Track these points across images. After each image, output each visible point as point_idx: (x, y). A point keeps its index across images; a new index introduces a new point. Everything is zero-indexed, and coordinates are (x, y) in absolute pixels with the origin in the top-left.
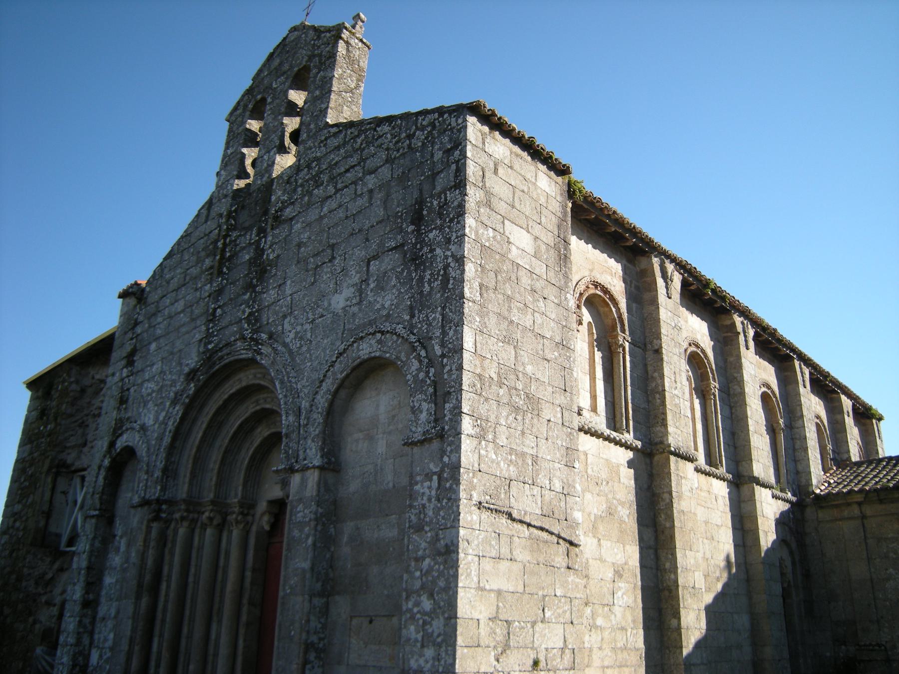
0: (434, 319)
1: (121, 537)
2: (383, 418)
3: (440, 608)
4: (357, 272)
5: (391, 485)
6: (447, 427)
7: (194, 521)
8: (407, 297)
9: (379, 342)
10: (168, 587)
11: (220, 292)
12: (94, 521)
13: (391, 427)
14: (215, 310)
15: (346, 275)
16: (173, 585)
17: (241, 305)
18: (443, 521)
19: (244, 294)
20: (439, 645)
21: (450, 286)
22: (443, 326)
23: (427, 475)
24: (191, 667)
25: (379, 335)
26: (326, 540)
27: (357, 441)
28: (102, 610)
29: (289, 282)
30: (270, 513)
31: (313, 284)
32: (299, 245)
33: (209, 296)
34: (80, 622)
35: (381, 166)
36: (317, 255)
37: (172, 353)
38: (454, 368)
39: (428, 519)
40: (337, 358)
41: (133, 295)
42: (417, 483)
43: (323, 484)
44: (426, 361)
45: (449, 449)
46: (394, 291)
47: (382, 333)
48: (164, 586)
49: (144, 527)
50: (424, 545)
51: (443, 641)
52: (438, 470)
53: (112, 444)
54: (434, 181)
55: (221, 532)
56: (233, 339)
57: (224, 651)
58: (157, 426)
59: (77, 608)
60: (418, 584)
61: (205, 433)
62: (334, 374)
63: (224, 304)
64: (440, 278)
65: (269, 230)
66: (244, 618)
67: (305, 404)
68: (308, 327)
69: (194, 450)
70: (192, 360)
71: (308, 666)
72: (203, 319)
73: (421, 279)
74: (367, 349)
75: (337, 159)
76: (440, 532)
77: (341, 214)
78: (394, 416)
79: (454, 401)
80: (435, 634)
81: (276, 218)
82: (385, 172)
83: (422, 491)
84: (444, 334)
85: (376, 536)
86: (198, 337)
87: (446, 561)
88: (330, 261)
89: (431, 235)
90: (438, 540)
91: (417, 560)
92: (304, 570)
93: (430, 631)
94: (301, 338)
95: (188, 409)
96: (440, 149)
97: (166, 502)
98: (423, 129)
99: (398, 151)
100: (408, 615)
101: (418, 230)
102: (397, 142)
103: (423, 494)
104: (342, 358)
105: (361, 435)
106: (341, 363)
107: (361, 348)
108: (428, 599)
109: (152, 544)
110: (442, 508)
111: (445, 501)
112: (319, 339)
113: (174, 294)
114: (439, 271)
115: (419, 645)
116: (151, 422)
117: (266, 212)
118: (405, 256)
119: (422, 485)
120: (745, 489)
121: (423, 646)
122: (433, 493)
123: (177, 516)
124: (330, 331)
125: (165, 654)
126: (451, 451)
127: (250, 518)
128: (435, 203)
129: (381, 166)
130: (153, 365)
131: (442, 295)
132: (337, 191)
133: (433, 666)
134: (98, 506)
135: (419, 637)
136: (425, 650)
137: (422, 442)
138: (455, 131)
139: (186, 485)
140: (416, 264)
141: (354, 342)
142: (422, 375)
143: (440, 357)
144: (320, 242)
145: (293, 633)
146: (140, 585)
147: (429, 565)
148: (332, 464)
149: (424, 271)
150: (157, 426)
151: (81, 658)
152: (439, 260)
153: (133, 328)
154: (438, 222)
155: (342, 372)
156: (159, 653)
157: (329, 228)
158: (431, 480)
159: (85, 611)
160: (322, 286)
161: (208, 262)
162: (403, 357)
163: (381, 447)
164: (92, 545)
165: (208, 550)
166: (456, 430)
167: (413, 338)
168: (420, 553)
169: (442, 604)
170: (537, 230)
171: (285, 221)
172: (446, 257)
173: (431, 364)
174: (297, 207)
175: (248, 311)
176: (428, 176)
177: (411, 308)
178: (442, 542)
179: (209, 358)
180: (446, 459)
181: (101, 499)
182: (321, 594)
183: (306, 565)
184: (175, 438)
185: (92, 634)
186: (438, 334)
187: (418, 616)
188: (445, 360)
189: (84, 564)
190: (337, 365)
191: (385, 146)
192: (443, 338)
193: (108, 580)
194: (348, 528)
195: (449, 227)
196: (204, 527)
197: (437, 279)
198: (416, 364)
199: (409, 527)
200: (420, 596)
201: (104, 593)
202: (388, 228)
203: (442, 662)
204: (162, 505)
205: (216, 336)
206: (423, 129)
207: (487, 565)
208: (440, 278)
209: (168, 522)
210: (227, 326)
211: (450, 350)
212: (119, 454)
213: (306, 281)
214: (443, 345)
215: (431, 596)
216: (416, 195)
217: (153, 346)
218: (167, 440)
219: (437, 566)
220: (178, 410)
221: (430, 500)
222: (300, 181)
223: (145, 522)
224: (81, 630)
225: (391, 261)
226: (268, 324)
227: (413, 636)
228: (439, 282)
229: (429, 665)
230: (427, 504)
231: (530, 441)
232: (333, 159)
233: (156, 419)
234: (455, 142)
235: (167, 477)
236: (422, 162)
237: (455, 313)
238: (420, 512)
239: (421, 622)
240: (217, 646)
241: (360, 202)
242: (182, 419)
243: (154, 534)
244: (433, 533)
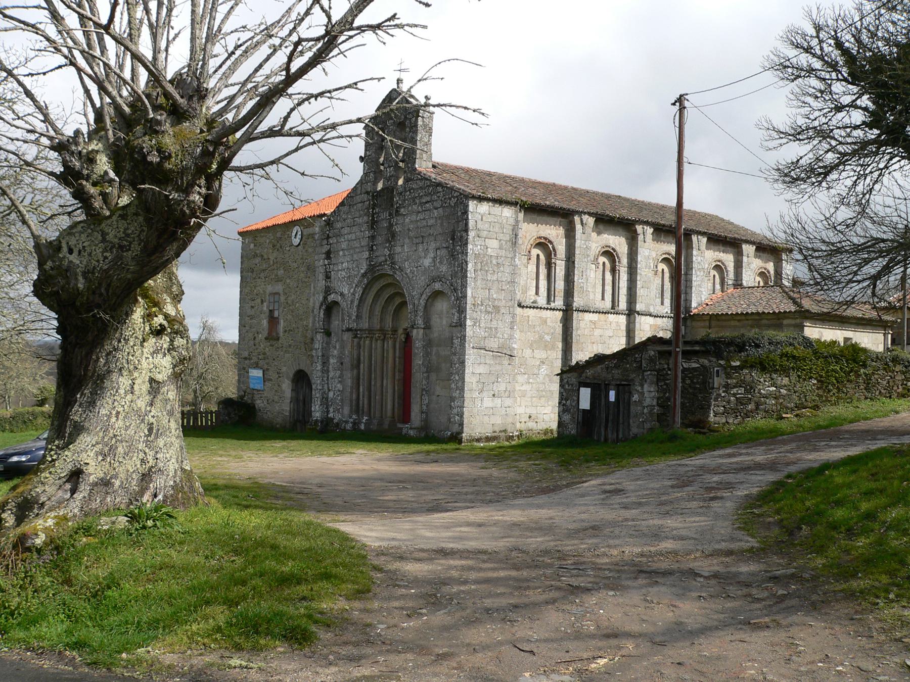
2: (445, 311)
16: (366, 365)
26: (427, 354)
28: (331, 374)
43: (425, 334)
48: (362, 365)
53: (325, 298)
57: (390, 391)
59: (320, 374)
66: (397, 377)
67: (416, 302)
74: (437, 286)
81: (397, 211)
120: (632, 317)
125: (366, 393)
146: (352, 365)
148: (428, 327)
165: (379, 350)
170: (501, 236)
179: (371, 268)
182: (426, 372)
183: (421, 363)
184: (360, 302)
189: (320, 354)
193: (332, 361)
194: (434, 349)
196: (377, 340)
206: (454, 197)
207: (476, 366)
218: (356, 303)
220: (360, 290)
225: (444, 252)
231: (494, 322)
240: (387, 389)
243: (355, 343)
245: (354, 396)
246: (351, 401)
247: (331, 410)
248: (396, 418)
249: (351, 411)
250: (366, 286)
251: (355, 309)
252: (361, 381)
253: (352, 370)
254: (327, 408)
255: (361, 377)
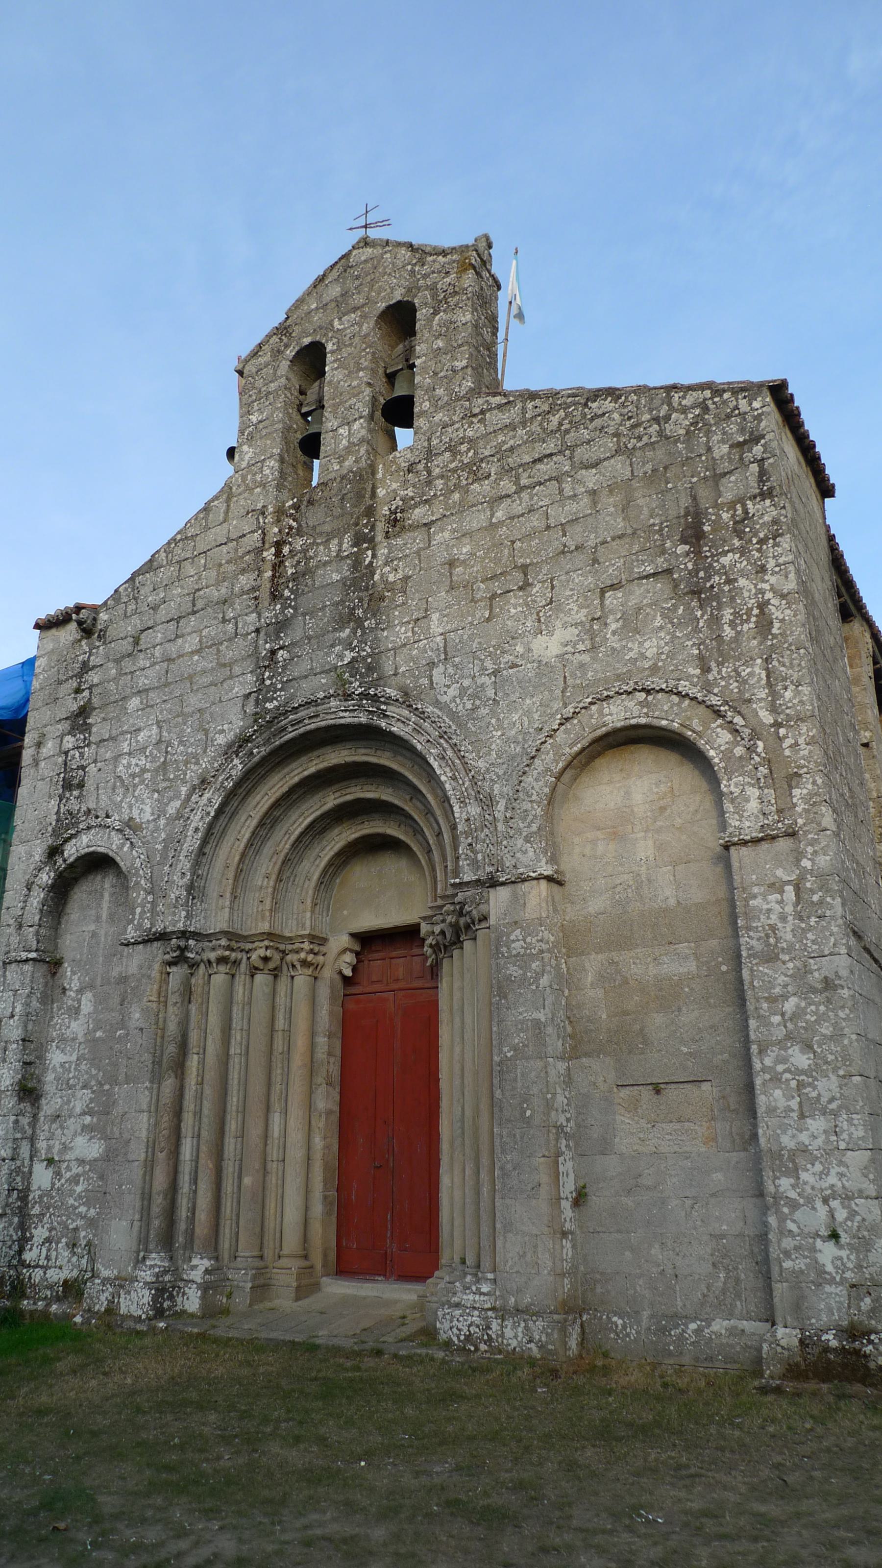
0: (751, 674)
1: (81, 991)
3: (827, 1063)
4: (581, 607)
5: (672, 902)
6: (800, 821)
7: (236, 963)
8: (690, 643)
9: (642, 704)
10: (202, 1062)
11: (281, 626)
12: (27, 967)
13: (659, 823)
14: (273, 652)
15: (559, 609)
17: (333, 646)
18: (814, 947)
19: (342, 629)
20: (835, 1114)
21: (775, 631)
22: (769, 685)
23: (772, 885)
24: (247, 1181)
25: (643, 695)
27: (594, 842)
29: (435, 617)
30: (351, 951)
31: (488, 620)
32: (451, 564)
33: (257, 631)
34: (16, 1122)
35: (608, 458)
36: (491, 578)
37: (182, 714)
38: (801, 741)
39: (784, 945)
40: (561, 724)
41: (80, 621)
42: (755, 897)
44: (747, 731)
45: (810, 849)
46: (662, 634)
47: (648, 692)
48: (193, 1062)
49: (155, 973)
50: (782, 979)
51: (840, 1107)
52: (794, 877)
53: (54, 852)
54: (717, 485)
55: (276, 976)
56: (321, 695)
57: (296, 1154)
58: (162, 822)
60: (779, 1033)
61: (253, 833)
62: (556, 748)
63: (293, 644)
64: (753, 619)
65: (379, 537)
68: (487, 681)
69: (237, 858)
70: (232, 724)
71: (561, 1159)
72: (249, 665)
73: (715, 620)
75: (512, 442)
76: (811, 961)
77: (536, 521)
78: (663, 809)
79: (810, 786)
80: (824, 1100)
82: (619, 467)
83: (765, 907)
84: (774, 694)
85: (653, 970)
86: (239, 690)
87: (829, 1000)
88: (521, 588)
89: (726, 560)
90: (808, 971)
91: (772, 1000)
92: (537, 1023)
93: (814, 1094)
94: (475, 696)
95: (230, 797)
96: (723, 441)
97: (197, 935)
98: (684, 411)
99: (639, 438)
100: (767, 1077)
101: (698, 553)
102: (633, 427)
103: (769, 911)
104: (568, 725)
105: (600, 835)
106: (566, 732)
107: (606, 711)
108: (802, 1052)
109: (173, 999)
110: (810, 928)
111: (813, 920)
112: (513, 697)
113: (172, 626)
114: (752, 609)
115: (795, 1115)
116: (148, 816)
117: (370, 512)
118: (676, 586)
119: (765, 899)
121: (802, 1116)
122: (789, 909)
123: (213, 956)
124: (535, 687)
125: (207, 1165)
126: (815, 852)
127: (320, 959)
128: (725, 516)
129: (608, 458)
130: (139, 730)
131: (760, 643)
132: (521, 489)
133: (827, 1141)
134: (34, 947)
135: (794, 1104)
136: (809, 1121)
137: (756, 841)
138: (749, 418)
139: (227, 910)
140: (700, 599)
141: (591, 703)
142: (739, 751)
143: (772, 726)
144: (497, 561)
145: (528, 1113)
146: (157, 1062)
147: (797, 1006)
149: (719, 608)
150: (162, 822)
151: (19, 1179)
152: (746, 594)
153: (80, 675)
154: (737, 543)
155: (571, 746)
156: (196, 1160)
157: (513, 542)
158: (782, 892)
159: (22, 1106)
160: (509, 623)
161: (245, 581)
162: (696, 724)
163: (645, 849)
164: (27, 1004)
165: (260, 1008)
166: (819, 824)
167: (715, 700)
168: (777, 990)
169: (830, 1058)
171: (414, 527)
172: (762, 592)
173: (755, 735)
174: (439, 510)
175: (349, 656)
176: (705, 478)
177: (701, 658)
178: (816, 974)
179: (267, 723)
180: (806, 863)
181: (37, 933)
184: (205, 841)
185: (32, 1140)
186: (764, 696)
187: (787, 1076)
188: (782, 731)
190: (560, 736)
191: (611, 430)
192: (773, 701)
195: (759, 550)
196: (254, 971)
197: (748, 621)
198: (725, 737)
199: (749, 956)
200: (786, 1049)
201: (50, 1077)
202: (636, 548)
203: (845, 1136)
204: (188, 939)
205: (281, 690)
206: (684, 411)
208: (753, 619)
209: (194, 965)
210: (306, 677)
211: (789, 718)
212: (71, 866)
213: (473, 616)
214: (774, 709)
215: (808, 1047)
216: (685, 502)
217: (134, 703)
218: (192, 842)
219: (813, 1008)
221: (783, 918)
222: (437, 470)
223: (157, 966)
224: (19, 1136)
226: (395, 675)
227: (782, 1103)
228: (752, 625)
229: (820, 1141)
230: (780, 925)
232: (504, 442)
233: (160, 812)
234: (751, 433)
235: (194, 898)
236: (688, 458)
237: (792, 666)
238: (767, 936)
239: (793, 1084)
241: (572, 507)
242: (220, 812)
244: (798, 964)
245: (160, 1180)
246: (147, 1197)
247: (39, 1233)
248: (317, 1261)
249: (143, 1242)
250: (238, 784)
251: (185, 864)
252: (188, 1119)
253: (156, 1078)
254: (23, 1227)
255: (189, 1104)
